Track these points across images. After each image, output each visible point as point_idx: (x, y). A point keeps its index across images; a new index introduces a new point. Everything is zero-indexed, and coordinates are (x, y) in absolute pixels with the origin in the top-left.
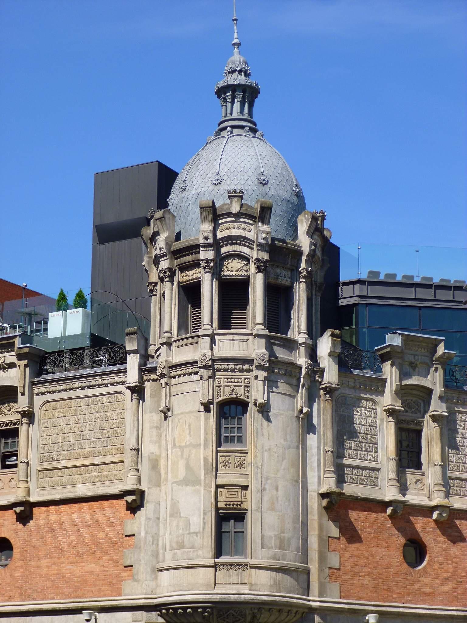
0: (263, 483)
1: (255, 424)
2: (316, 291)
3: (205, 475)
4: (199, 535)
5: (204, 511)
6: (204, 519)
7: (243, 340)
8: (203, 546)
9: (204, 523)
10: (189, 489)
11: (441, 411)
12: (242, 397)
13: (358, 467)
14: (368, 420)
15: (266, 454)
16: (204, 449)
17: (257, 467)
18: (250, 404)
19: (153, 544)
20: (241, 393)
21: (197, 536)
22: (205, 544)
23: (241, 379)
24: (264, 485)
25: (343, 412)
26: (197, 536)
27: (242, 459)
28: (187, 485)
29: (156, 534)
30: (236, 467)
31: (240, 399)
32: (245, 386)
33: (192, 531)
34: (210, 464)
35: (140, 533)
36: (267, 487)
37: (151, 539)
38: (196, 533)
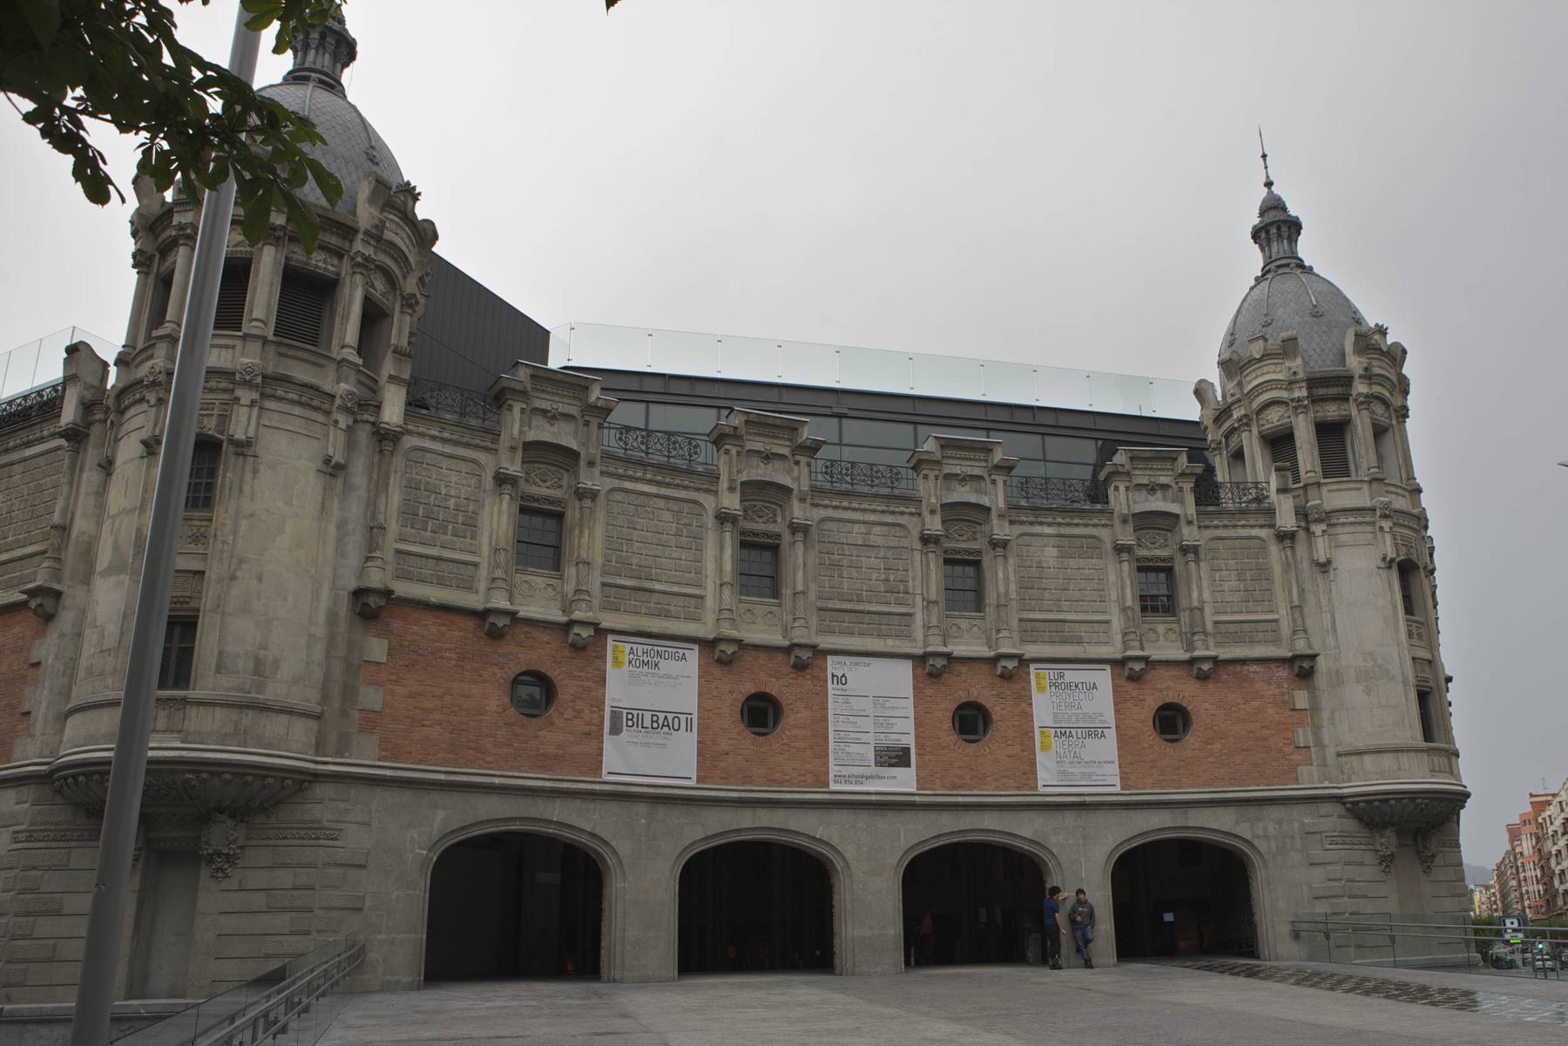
0: (233, 567)
1: (228, 475)
2: (402, 306)
3: (134, 555)
4: (112, 653)
5: (124, 613)
6: (122, 626)
7: (227, 347)
8: (114, 671)
9: (122, 633)
10: (112, 580)
11: (590, 483)
12: (210, 432)
13: (439, 559)
14: (463, 491)
15: (244, 524)
16: (140, 514)
17: (224, 542)
18: (225, 445)
19: (63, 676)
20: (211, 427)
21: (110, 655)
22: (119, 667)
23: (213, 404)
24: (235, 570)
25: (417, 474)
26: (110, 655)
27: (202, 530)
28: (109, 576)
29: (72, 659)
30: (190, 543)
31: (207, 435)
32: (219, 415)
33: (104, 648)
34: (144, 536)
35: (48, 659)
36: (239, 574)
37: (62, 668)
38: (109, 650)
